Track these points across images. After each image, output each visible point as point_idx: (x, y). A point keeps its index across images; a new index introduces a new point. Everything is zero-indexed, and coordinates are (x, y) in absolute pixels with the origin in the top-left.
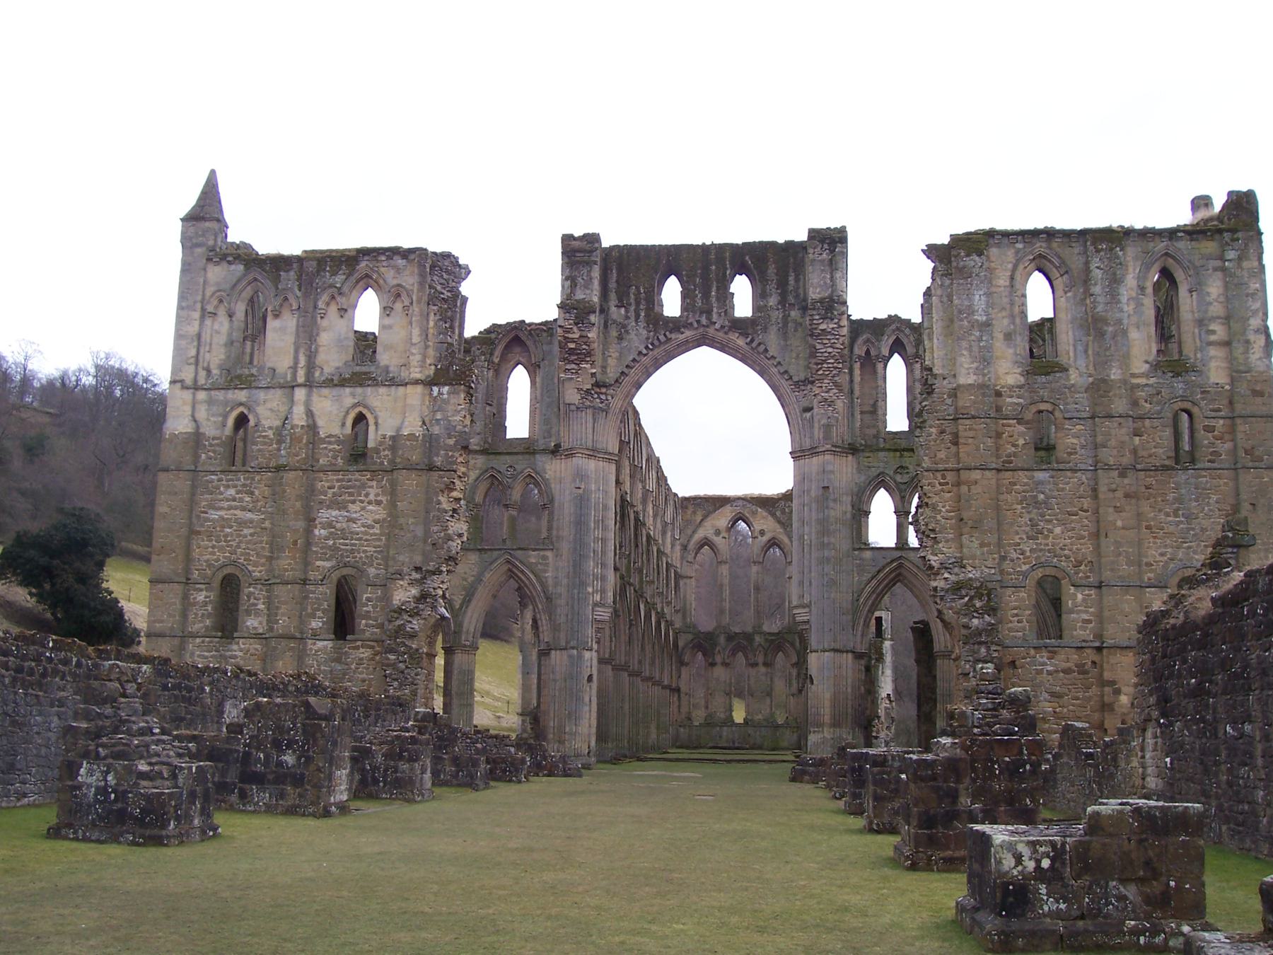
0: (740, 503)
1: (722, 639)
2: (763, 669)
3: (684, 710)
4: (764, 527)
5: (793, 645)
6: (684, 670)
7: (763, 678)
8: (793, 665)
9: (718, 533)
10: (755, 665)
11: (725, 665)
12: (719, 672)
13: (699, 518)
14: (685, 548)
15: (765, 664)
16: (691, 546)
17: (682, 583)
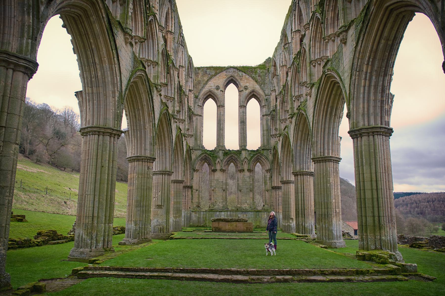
0: (232, 70)
1: (221, 154)
2: (247, 174)
3: (195, 200)
4: (247, 84)
5: (267, 158)
6: (196, 175)
7: (248, 180)
8: (267, 171)
9: (218, 88)
10: (242, 171)
11: (222, 171)
12: (218, 175)
13: (206, 79)
14: (196, 97)
15: (249, 170)
16: (201, 96)
17: (194, 118)
